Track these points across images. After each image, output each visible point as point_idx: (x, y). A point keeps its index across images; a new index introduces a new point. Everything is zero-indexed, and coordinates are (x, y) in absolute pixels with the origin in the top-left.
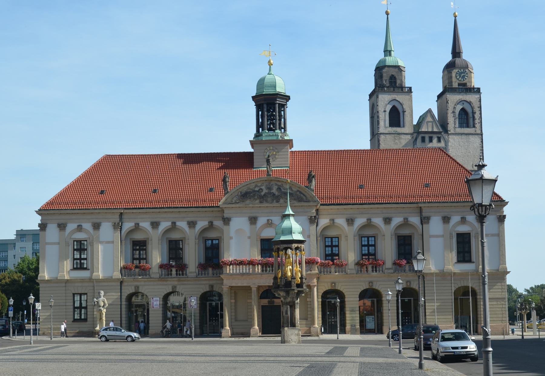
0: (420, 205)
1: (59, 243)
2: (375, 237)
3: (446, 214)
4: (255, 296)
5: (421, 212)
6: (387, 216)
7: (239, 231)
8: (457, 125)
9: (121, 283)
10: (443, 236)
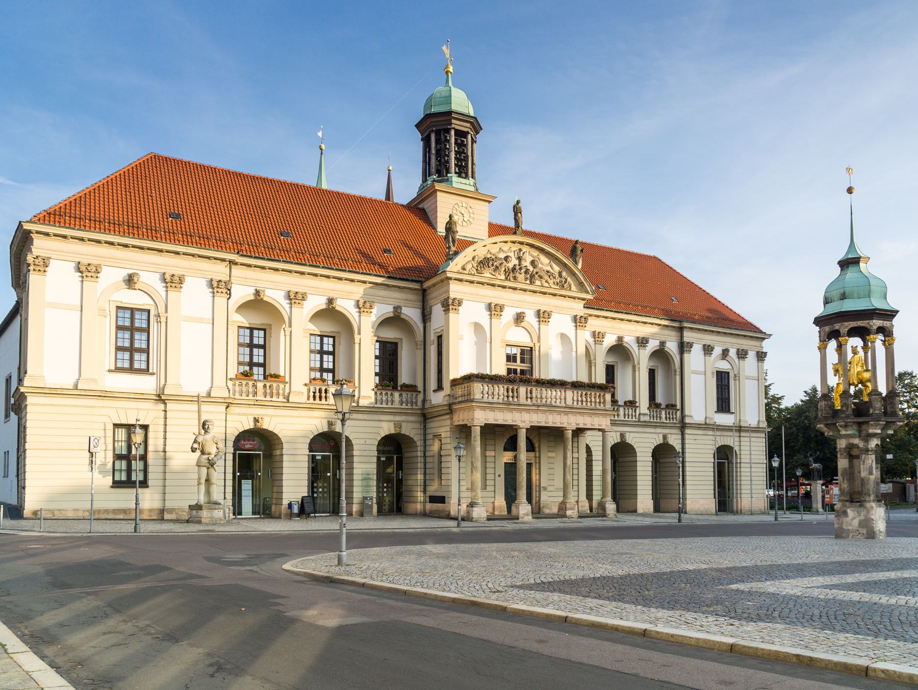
2: (265, 330)
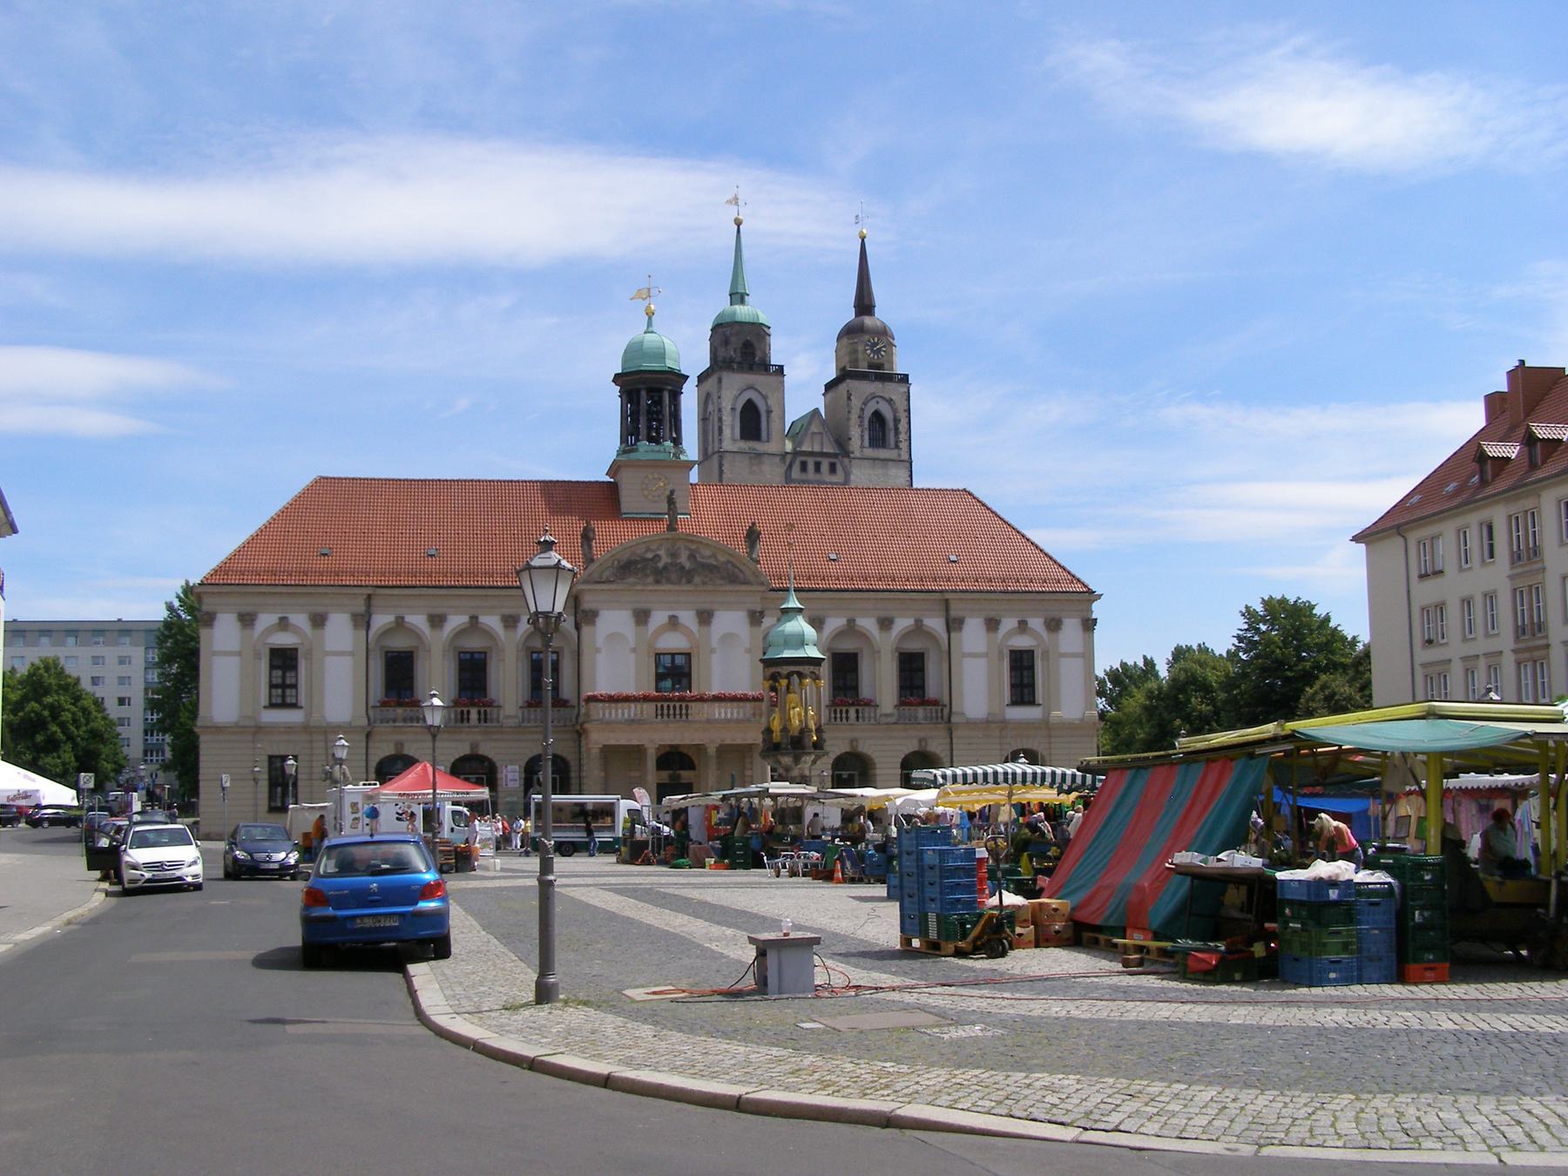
0: (947, 596)
1: (239, 654)
3: (992, 614)
4: (651, 763)
5: (947, 609)
6: (883, 614)
8: (867, 443)
9: (368, 735)
10: (986, 655)
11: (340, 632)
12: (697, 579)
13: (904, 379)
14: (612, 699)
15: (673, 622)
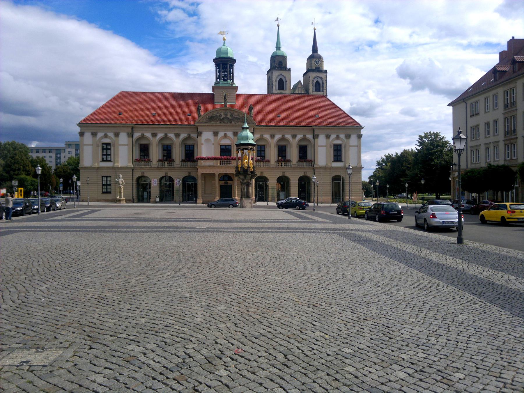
0: (314, 128)
4: (217, 178)
5: (314, 132)
6: (294, 133)
7: (208, 140)
9: (133, 170)
11: (123, 138)
12: (233, 123)
13: (326, 71)
14: (208, 159)
15: (226, 136)
